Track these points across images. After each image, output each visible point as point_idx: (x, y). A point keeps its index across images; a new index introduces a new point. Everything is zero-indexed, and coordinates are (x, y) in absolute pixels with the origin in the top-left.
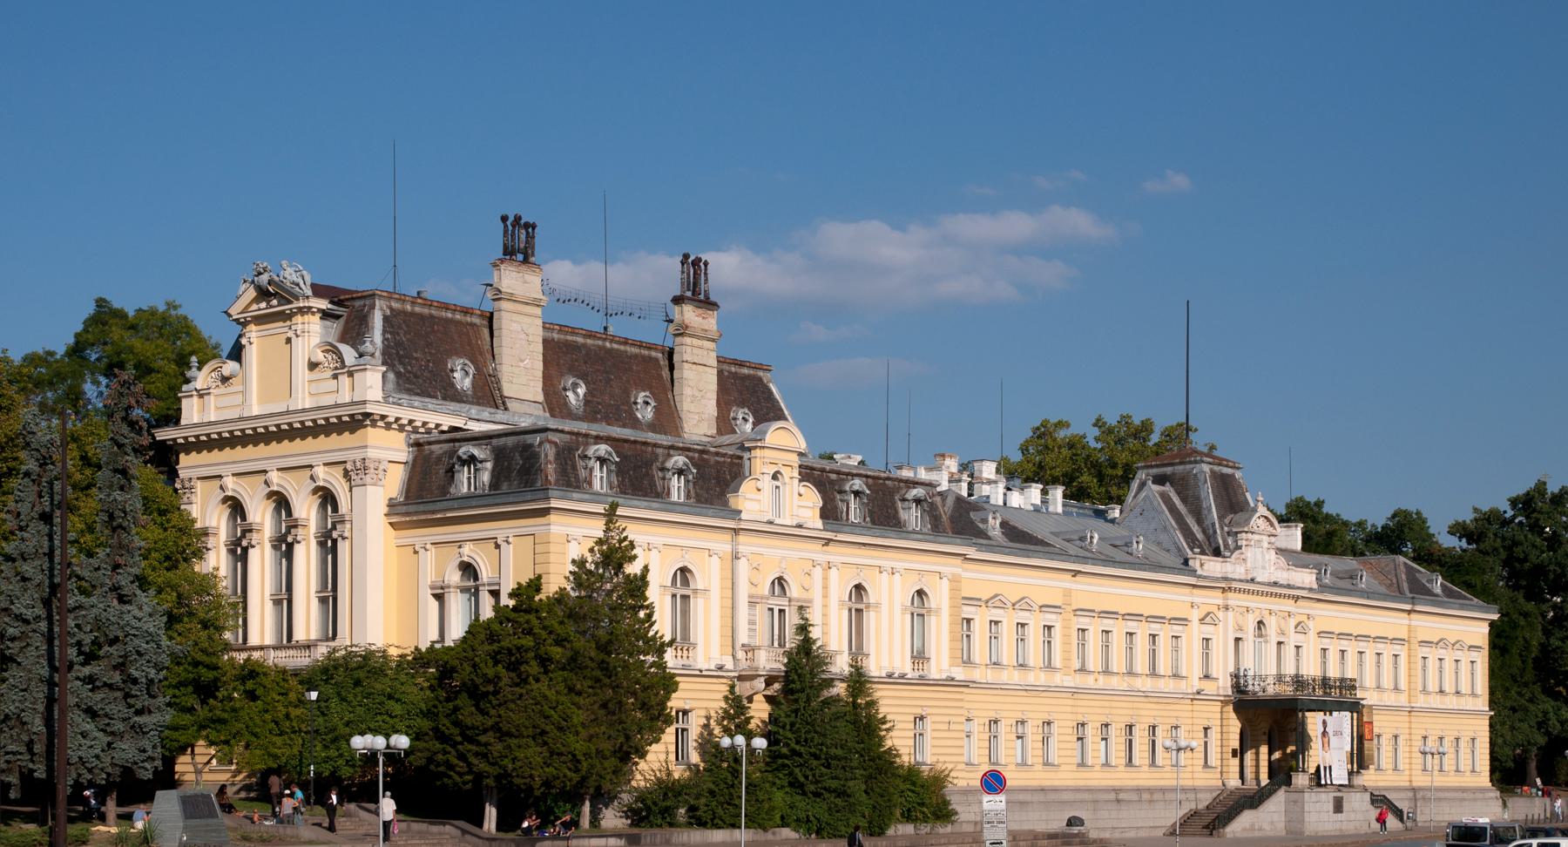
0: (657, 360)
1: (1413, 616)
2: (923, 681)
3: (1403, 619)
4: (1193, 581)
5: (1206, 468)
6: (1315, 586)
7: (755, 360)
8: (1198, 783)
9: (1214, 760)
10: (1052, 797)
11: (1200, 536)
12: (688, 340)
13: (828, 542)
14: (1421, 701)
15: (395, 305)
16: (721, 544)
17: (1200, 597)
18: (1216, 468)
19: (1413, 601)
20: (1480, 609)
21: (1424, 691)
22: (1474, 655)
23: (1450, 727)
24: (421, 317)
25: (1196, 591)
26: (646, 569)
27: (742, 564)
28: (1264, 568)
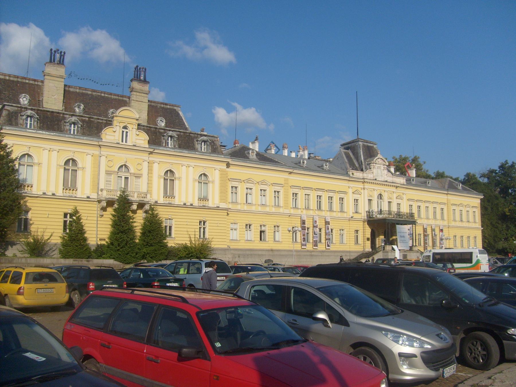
0: (126, 101)
1: (448, 195)
2: (204, 207)
3: (445, 197)
4: (348, 178)
5: (361, 143)
6: (405, 183)
7: (174, 103)
8: (351, 250)
9: (360, 241)
10: (276, 253)
11: (357, 165)
12: (135, 93)
13: (151, 153)
14: (453, 224)
16: (95, 151)
17: (352, 184)
18: (365, 144)
19: (448, 190)
20: (476, 194)
21: (455, 220)
22: (474, 210)
23: (466, 233)
24: (13, 81)
25: (350, 182)
26: (12, 151)
27: (103, 159)
28: (382, 176)
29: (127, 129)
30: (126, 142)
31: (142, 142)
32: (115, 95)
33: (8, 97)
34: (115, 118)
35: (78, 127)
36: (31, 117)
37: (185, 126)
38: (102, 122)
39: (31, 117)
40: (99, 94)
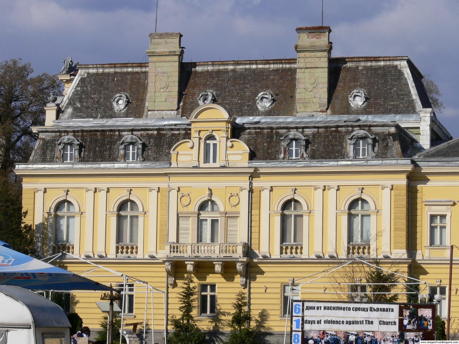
15: (91, 71)
27: (173, 194)
29: (215, 139)
30: (215, 161)
31: (239, 158)
32: (276, 61)
33: (98, 102)
34: (193, 125)
35: (138, 149)
36: (71, 144)
37: (411, 96)
38: (179, 134)
39: (71, 144)
40: (248, 66)
